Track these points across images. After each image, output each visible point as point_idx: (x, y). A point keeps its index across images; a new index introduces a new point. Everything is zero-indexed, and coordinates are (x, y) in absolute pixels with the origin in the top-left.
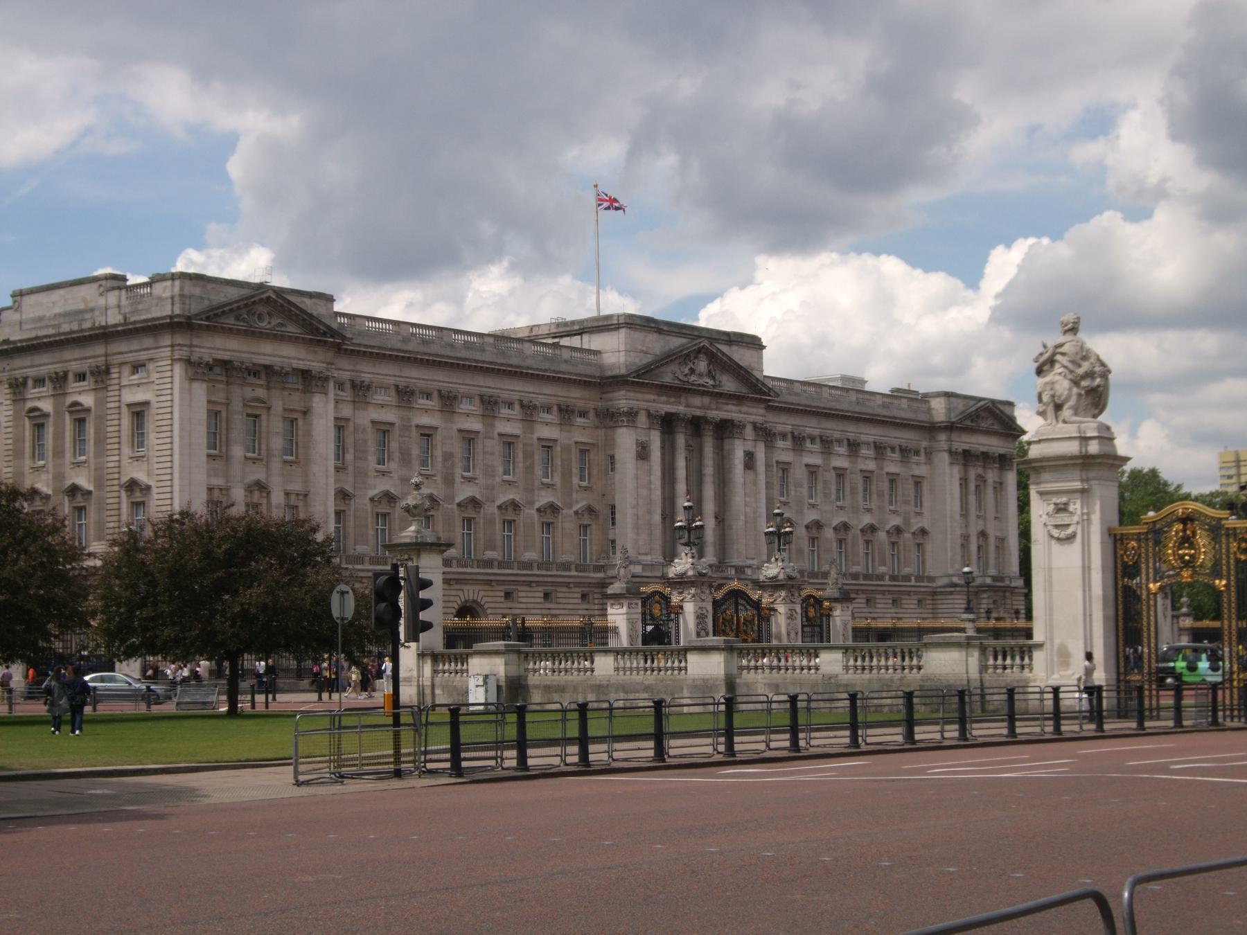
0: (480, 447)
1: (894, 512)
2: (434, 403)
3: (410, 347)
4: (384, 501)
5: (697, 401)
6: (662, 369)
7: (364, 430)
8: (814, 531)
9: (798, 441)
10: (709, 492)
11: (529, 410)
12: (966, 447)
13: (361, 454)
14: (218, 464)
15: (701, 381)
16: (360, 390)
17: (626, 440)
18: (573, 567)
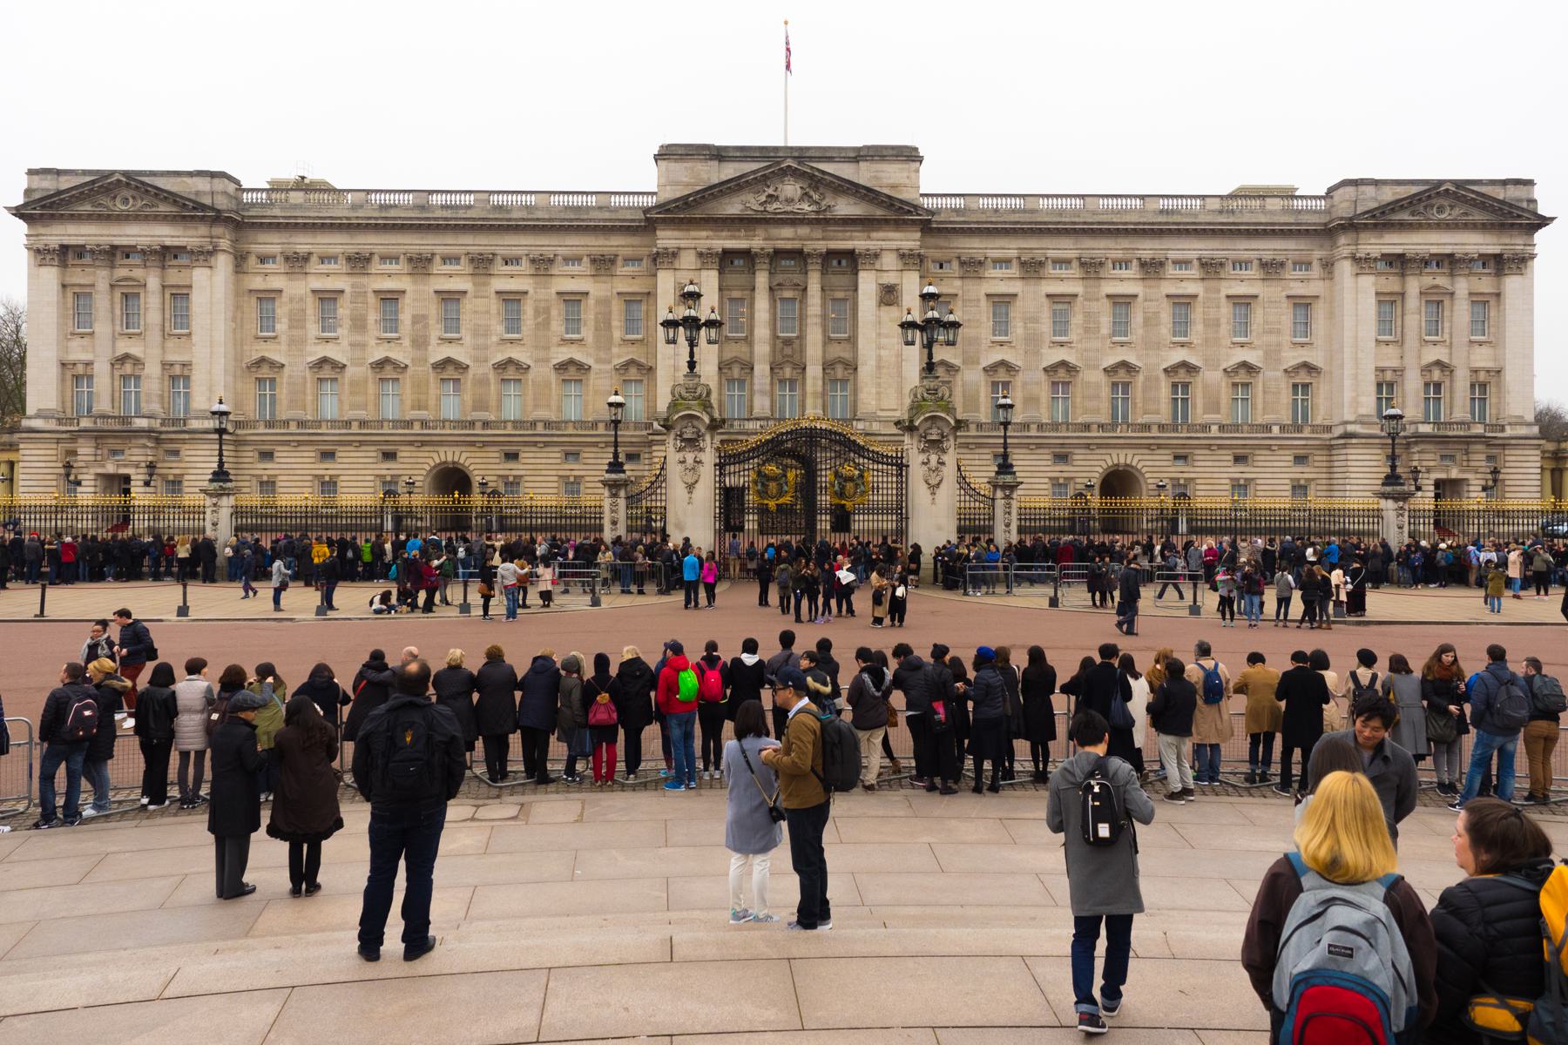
0: (468, 307)
1: (1242, 345)
2: (402, 266)
3: (360, 214)
4: (327, 367)
5: (787, 232)
7: (301, 299)
8: (1062, 373)
9: (1032, 268)
10: (814, 337)
11: (542, 265)
12: (1398, 250)
13: (297, 321)
14: (86, 341)
15: (789, 209)
16: (297, 262)
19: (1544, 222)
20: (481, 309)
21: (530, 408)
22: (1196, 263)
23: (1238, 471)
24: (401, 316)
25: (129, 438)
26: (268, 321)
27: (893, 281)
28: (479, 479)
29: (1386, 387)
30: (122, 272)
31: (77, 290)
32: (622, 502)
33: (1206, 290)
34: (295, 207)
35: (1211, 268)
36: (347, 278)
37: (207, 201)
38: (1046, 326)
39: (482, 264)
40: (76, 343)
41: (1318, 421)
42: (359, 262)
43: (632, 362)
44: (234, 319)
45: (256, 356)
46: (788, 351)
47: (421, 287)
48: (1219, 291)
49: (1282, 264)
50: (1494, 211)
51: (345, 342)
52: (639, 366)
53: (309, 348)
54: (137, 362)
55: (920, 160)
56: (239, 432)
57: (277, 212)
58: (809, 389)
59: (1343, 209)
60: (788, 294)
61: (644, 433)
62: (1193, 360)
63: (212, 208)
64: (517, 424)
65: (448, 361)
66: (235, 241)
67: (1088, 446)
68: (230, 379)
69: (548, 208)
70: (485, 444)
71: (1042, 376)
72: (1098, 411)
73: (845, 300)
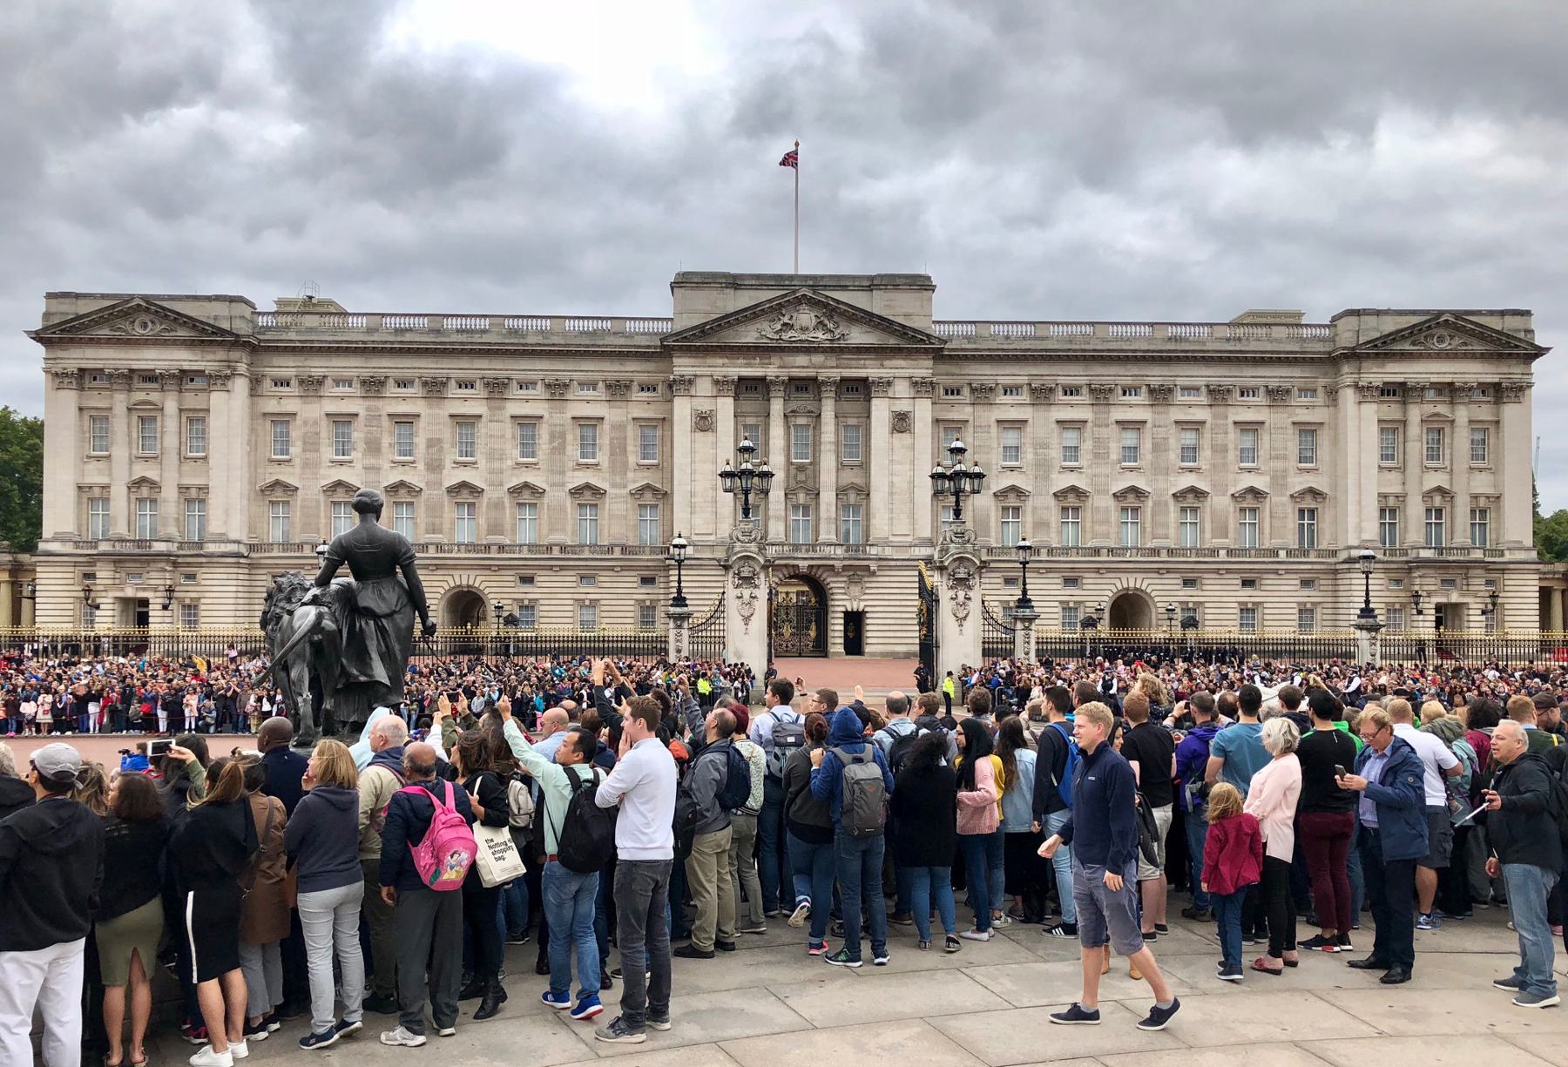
0: (483, 431)
1: (1250, 471)
3: (376, 337)
4: (340, 490)
5: (802, 360)
6: (741, 328)
7: (316, 423)
8: (1072, 500)
9: (1042, 395)
10: (828, 462)
11: (557, 390)
12: (1399, 379)
13: (311, 444)
14: (101, 465)
15: (803, 337)
16: (312, 385)
17: (683, 409)
18: (617, 550)
19: (1540, 352)
20: (497, 432)
21: (545, 532)
22: (1204, 389)
23: (1247, 595)
24: (416, 440)
25: (148, 562)
26: (284, 443)
27: (905, 409)
28: (494, 602)
29: (1389, 511)
30: (141, 396)
31: (93, 413)
32: (685, 633)
33: (1215, 417)
34: (311, 330)
35: (1218, 395)
36: (360, 401)
37: (225, 325)
38: (1055, 453)
39: (497, 388)
40: (93, 466)
41: (1324, 546)
42: (373, 386)
43: (648, 487)
44: (249, 443)
45: (270, 479)
46: (801, 477)
47: (437, 411)
48: (1226, 417)
49: (1288, 391)
50: (1491, 341)
51: (358, 466)
52: (654, 490)
53: (322, 471)
54: (154, 485)
55: (932, 289)
56: (253, 555)
57: (293, 336)
58: (823, 514)
59: (1346, 339)
60: (802, 421)
61: (661, 557)
62: (1202, 486)
63: (230, 333)
64: (532, 547)
65: (464, 485)
66: (250, 365)
67: (1098, 571)
68: (245, 502)
69: (564, 334)
70: (501, 568)
71: (1052, 502)
72: (1107, 535)
73: (857, 427)
